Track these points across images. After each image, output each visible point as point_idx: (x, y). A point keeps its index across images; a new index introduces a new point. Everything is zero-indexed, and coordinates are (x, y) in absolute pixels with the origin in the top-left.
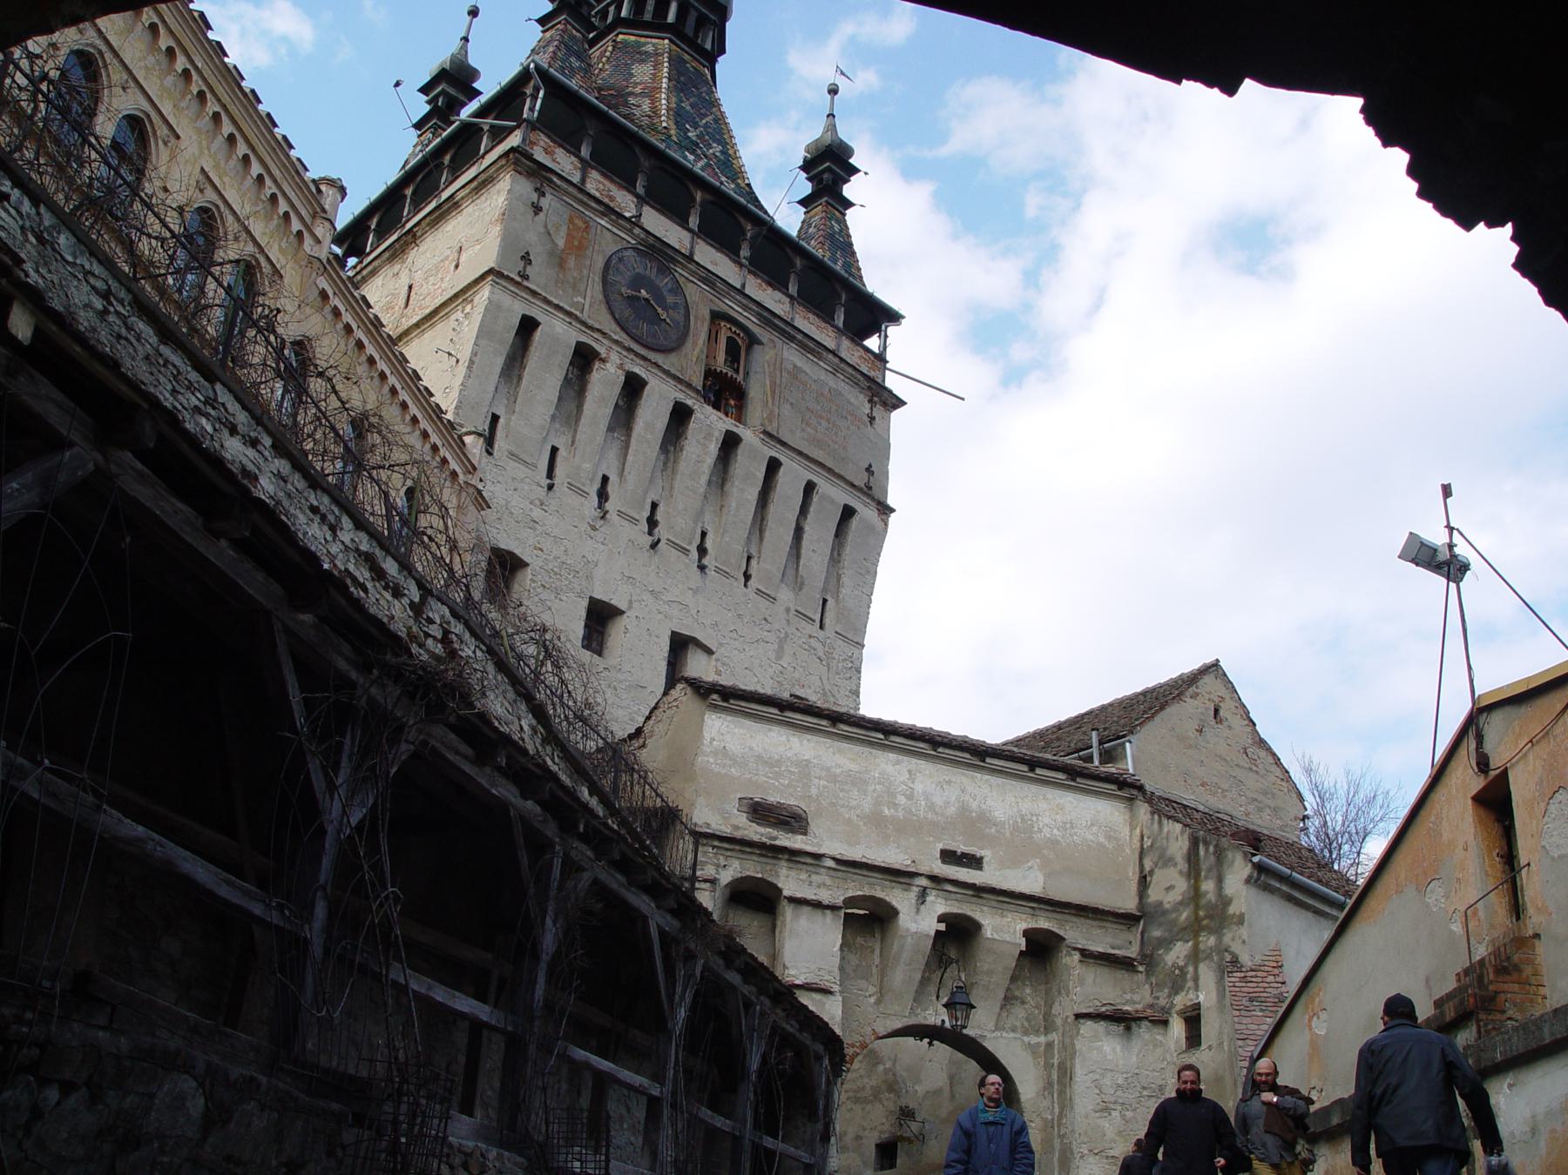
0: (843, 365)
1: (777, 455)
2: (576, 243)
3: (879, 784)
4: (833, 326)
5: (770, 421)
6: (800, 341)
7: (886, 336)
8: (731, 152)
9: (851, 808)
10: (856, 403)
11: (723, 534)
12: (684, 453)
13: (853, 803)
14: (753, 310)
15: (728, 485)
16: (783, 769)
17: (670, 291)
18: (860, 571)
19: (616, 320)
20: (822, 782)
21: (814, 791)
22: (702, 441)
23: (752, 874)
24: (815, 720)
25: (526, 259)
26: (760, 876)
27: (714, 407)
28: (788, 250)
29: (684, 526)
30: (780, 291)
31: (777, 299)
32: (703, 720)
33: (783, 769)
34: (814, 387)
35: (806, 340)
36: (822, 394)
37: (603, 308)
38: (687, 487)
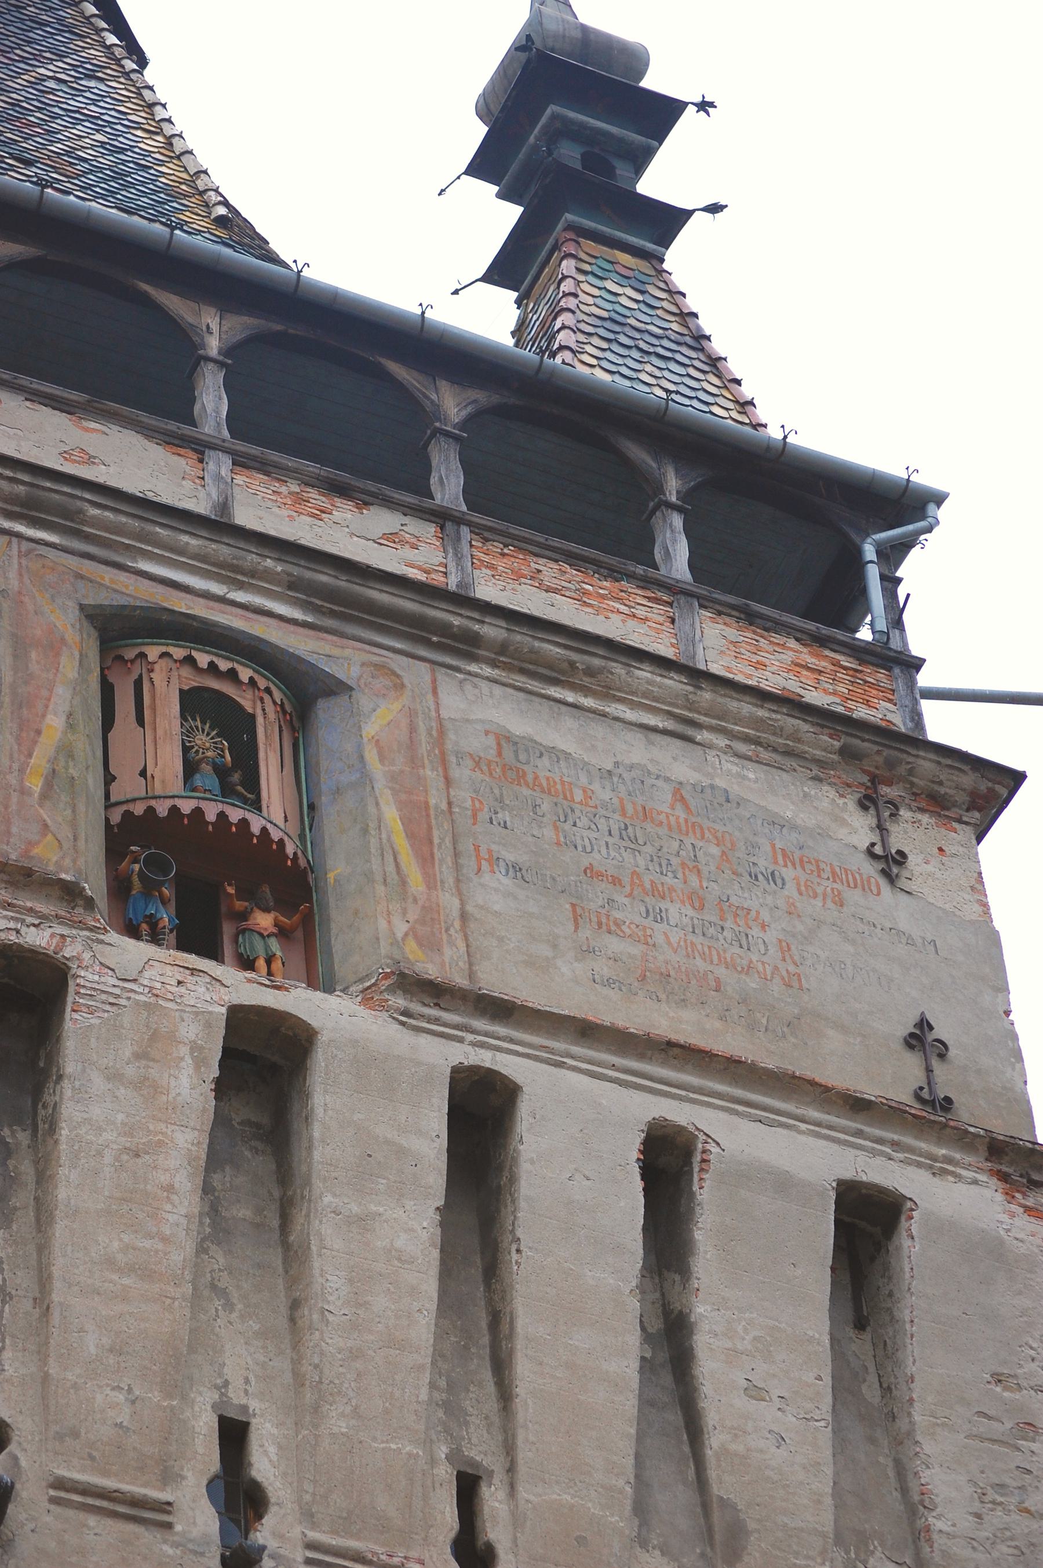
0: (706, 696)
1: (485, 1059)
4: (646, 583)
5: (431, 945)
6: (503, 648)
7: (891, 582)
8: (152, 144)
10: (806, 818)
11: (316, 1409)
12: (64, 1132)
14: (267, 575)
15: (299, 1219)
18: (984, 1426)
22: (130, 1071)
27: (182, 946)
28: (394, 368)
29: (124, 1418)
30: (388, 503)
31: (377, 533)
34: (603, 793)
35: (522, 638)
36: (646, 814)
38: (110, 1262)
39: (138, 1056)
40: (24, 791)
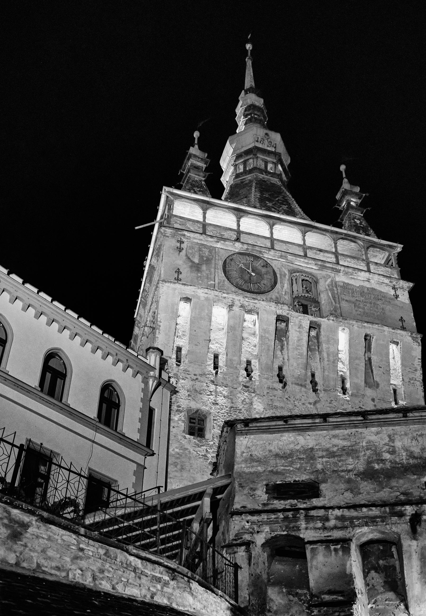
2: (205, 259)
3: (367, 449)
9: (349, 471)
13: (350, 467)
14: (312, 263)
16: (295, 458)
17: (263, 266)
19: (235, 286)
20: (324, 460)
21: (319, 467)
23: (279, 533)
24: (310, 421)
25: (178, 272)
26: (285, 533)
32: (235, 443)
33: (295, 458)
37: (227, 282)
39: (299, 328)
40: (282, 294)
